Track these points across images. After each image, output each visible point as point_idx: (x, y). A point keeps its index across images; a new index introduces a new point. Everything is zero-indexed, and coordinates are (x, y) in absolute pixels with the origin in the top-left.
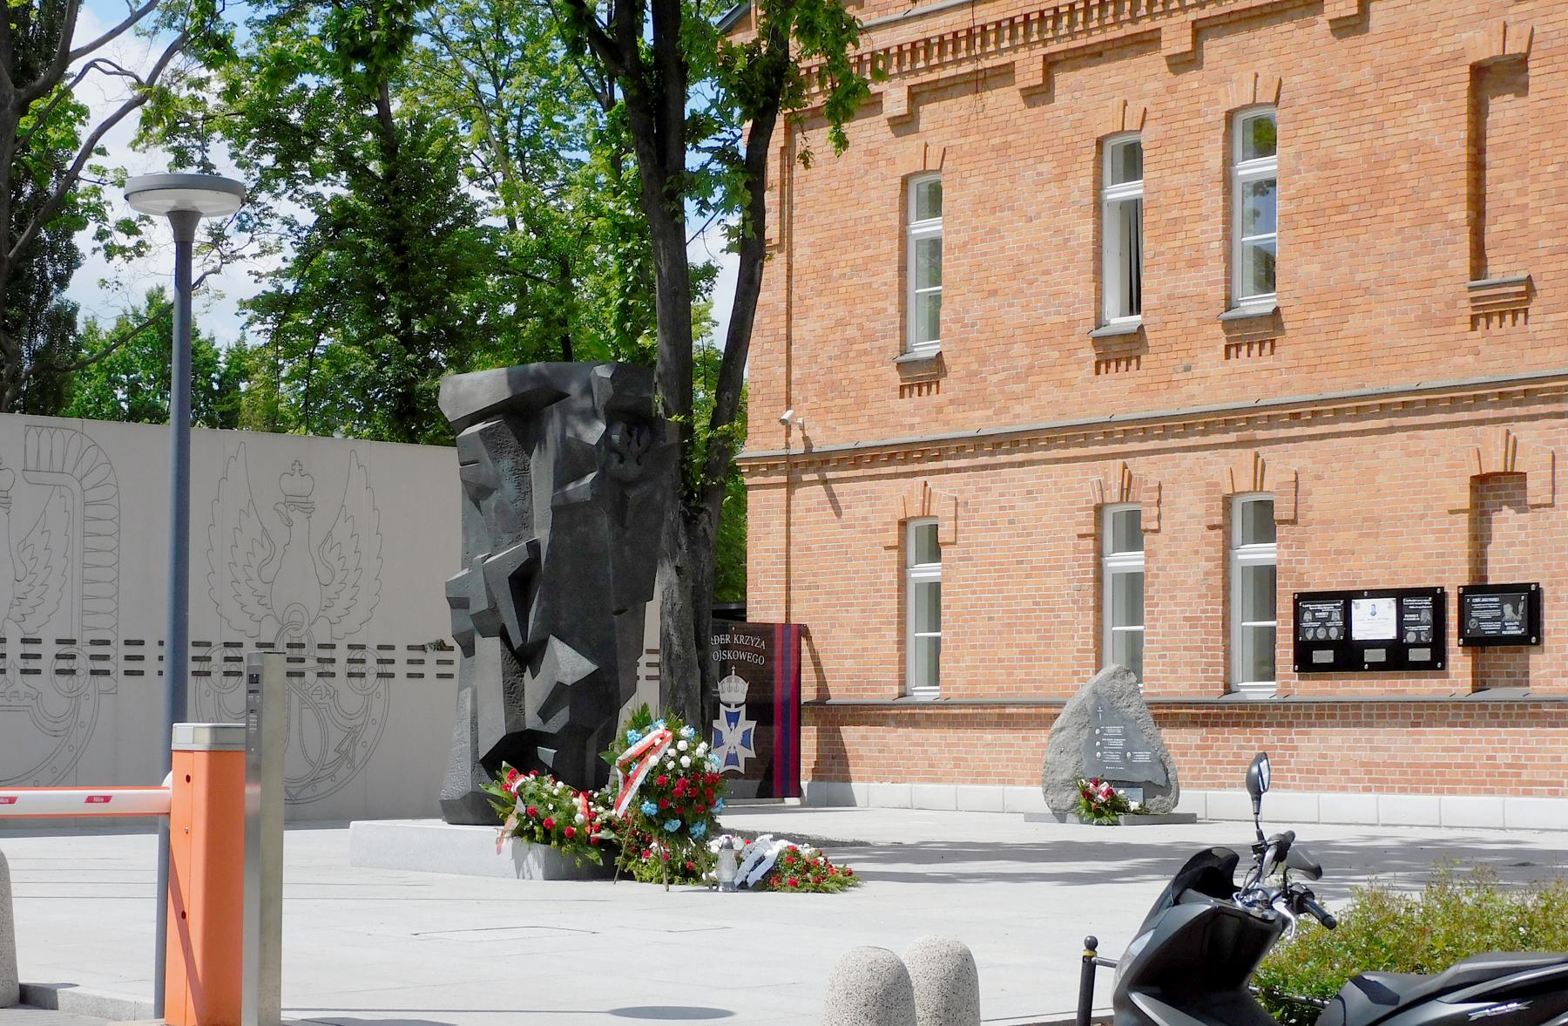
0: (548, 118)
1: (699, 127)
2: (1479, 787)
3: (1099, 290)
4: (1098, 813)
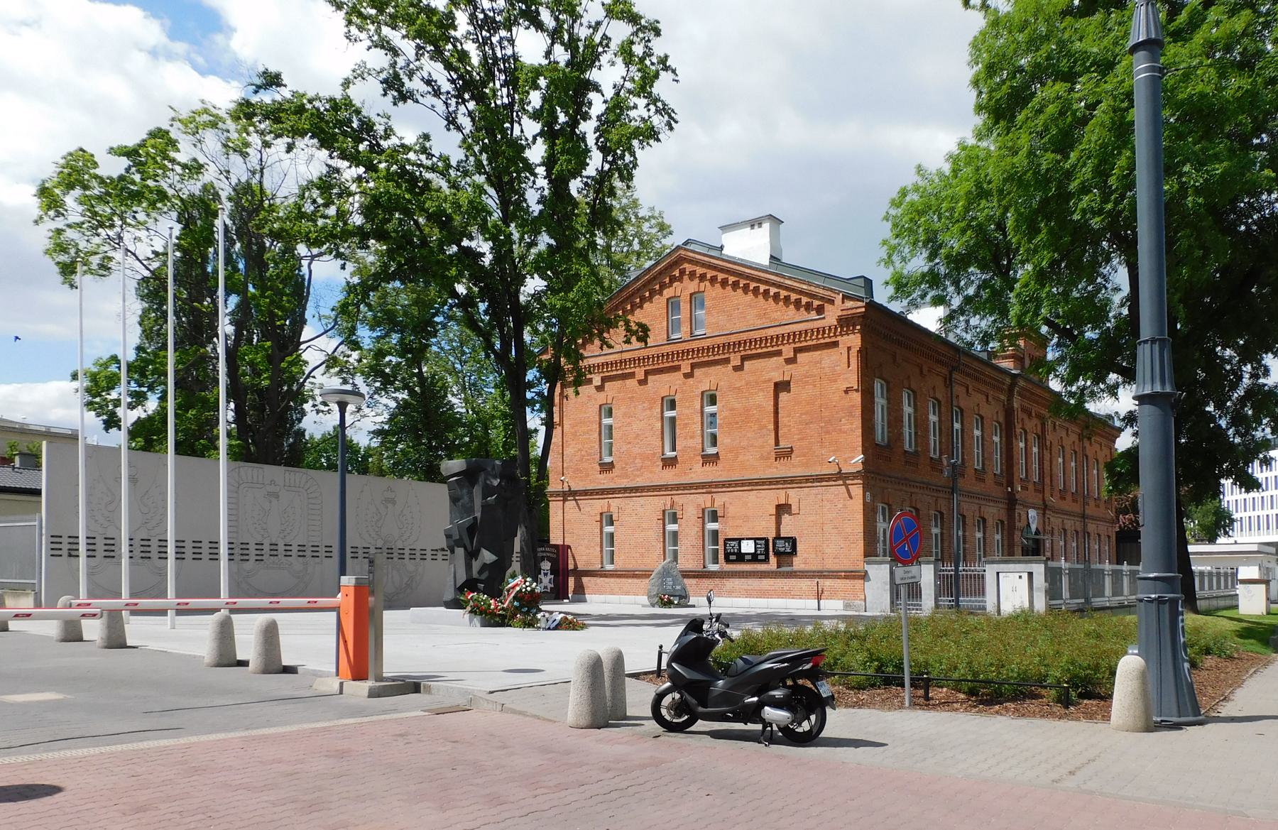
0: (480, 378)
1: (530, 385)
2: (779, 597)
3: (663, 444)
4: (665, 605)
